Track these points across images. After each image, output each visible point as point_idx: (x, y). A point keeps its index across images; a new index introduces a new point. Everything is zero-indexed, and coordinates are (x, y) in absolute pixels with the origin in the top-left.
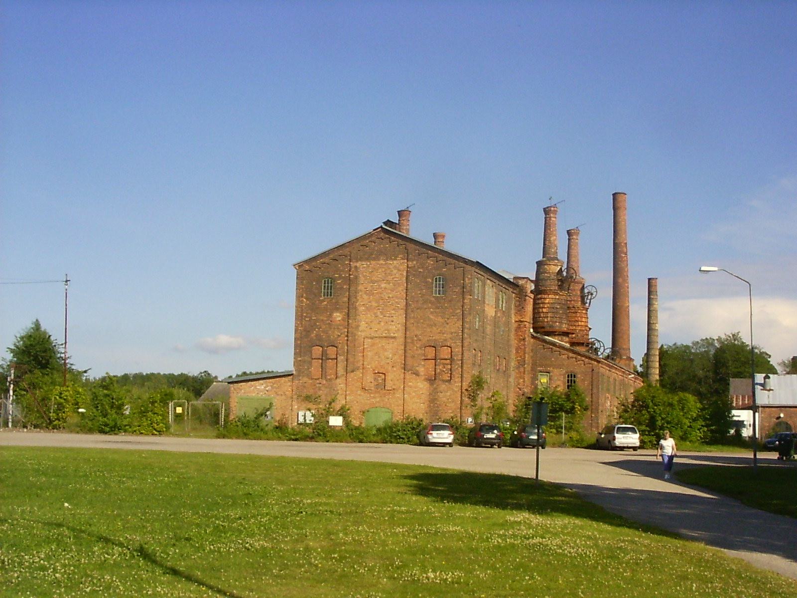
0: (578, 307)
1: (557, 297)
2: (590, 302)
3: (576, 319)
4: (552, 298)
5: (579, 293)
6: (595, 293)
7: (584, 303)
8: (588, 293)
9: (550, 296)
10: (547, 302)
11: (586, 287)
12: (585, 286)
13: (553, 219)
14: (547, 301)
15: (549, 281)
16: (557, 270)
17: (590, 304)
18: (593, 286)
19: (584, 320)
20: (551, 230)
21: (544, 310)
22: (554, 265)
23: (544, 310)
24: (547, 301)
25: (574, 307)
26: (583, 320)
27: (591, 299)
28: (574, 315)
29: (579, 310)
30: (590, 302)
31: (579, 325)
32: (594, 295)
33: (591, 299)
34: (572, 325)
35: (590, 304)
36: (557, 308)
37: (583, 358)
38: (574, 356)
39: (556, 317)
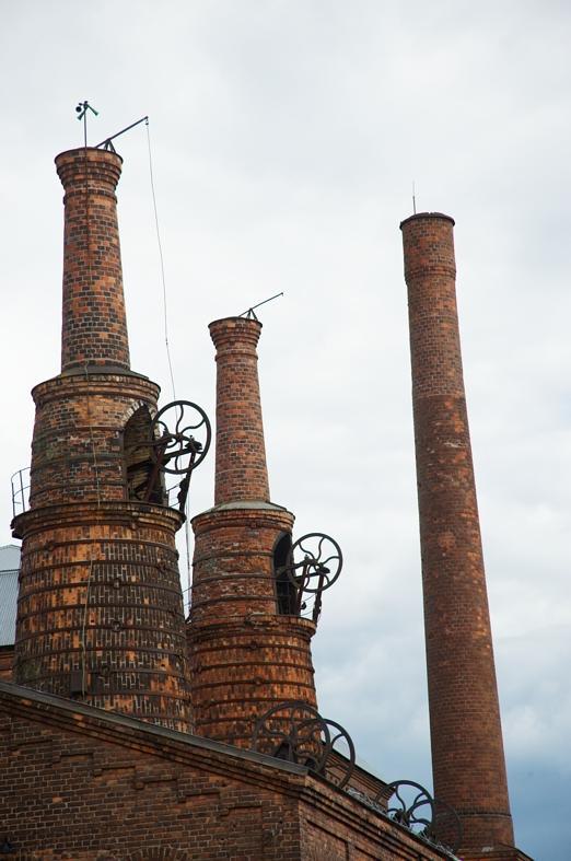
0: (266, 624)
1: (129, 536)
2: (318, 603)
3: (261, 672)
4: (102, 542)
5: (267, 565)
6: (332, 566)
7: (290, 604)
8: (307, 562)
10: (80, 558)
11: (299, 542)
12: (294, 540)
13: (98, 201)
14: (81, 554)
15: (85, 466)
16: (126, 418)
17: (317, 612)
18: (324, 536)
19: (292, 675)
20: (94, 247)
21: (70, 597)
22: (106, 395)
23: (70, 597)
24: (81, 554)
25: (248, 624)
26: (289, 678)
27: (321, 588)
28: (250, 657)
29: (268, 634)
30: (318, 603)
32: (331, 576)
33: (318, 592)
34: (241, 701)
35: (317, 612)
36: (128, 584)
37: (213, 779)
38: (166, 770)
39: (125, 628)
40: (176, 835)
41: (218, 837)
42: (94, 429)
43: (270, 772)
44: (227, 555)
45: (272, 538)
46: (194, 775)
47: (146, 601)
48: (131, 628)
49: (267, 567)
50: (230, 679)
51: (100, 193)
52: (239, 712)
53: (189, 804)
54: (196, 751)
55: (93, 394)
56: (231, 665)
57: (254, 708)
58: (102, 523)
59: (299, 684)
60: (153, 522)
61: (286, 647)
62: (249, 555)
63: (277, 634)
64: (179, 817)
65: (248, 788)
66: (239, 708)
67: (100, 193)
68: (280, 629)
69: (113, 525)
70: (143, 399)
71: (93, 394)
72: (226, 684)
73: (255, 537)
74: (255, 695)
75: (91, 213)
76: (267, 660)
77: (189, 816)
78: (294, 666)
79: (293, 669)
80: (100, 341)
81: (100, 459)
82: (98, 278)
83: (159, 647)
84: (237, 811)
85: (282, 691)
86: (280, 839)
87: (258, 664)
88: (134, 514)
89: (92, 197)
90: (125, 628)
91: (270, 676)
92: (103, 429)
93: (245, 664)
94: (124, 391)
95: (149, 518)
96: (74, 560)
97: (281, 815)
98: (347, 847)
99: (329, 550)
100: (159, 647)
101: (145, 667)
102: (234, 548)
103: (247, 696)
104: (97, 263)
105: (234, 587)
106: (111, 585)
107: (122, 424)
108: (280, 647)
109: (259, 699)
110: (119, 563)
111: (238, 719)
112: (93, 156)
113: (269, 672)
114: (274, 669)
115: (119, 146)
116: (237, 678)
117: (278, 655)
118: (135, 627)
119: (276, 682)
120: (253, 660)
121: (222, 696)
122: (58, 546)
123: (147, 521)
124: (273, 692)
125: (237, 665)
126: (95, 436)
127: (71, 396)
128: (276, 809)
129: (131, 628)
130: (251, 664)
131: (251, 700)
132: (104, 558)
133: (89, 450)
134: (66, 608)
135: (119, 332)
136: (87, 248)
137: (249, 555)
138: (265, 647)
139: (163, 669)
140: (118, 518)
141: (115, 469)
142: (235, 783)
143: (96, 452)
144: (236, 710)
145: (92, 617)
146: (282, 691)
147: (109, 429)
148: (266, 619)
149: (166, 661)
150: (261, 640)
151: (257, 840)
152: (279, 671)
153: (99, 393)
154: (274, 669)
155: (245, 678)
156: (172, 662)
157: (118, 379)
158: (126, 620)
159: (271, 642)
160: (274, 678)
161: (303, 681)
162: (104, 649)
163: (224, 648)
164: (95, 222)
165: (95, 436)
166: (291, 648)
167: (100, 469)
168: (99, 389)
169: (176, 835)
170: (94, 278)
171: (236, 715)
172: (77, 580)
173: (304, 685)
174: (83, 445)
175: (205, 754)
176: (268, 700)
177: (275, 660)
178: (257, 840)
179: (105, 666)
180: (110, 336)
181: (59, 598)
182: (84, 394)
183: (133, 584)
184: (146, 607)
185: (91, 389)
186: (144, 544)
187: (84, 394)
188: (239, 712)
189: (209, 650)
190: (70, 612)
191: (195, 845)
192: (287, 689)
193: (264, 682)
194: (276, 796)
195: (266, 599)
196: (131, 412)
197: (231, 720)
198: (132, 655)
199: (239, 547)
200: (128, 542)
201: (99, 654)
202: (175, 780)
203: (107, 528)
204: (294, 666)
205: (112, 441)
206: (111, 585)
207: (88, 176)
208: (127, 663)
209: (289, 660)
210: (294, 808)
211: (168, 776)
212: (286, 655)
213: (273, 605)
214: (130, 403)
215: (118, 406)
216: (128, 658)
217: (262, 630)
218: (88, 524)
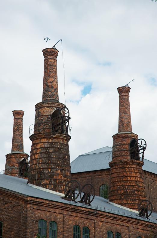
0: (126, 162)
1: (51, 141)
3: (125, 174)
4: (44, 143)
9: (43, 140)
10: (39, 147)
15: (42, 124)
16: (52, 112)
18: (143, 139)
20: (49, 72)
22: (47, 107)
25: (121, 162)
26: (133, 175)
28: (122, 170)
29: (127, 164)
31: (128, 181)
33: (143, 153)
34: (120, 181)
36: (50, 152)
37: (11, 199)
39: (48, 163)
40: (3, 213)
41: (11, 214)
42: (44, 115)
43: (21, 197)
44: (118, 145)
45: (130, 141)
46: (7, 198)
47: (54, 157)
48: (50, 163)
49: (128, 148)
50: (118, 176)
51: (51, 59)
52: (119, 184)
53: (6, 206)
54: (7, 192)
55: (44, 107)
56: (118, 172)
57: (123, 183)
58: (44, 138)
59: (135, 177)
60: (58, 137)
61: (132, 167)
62: (123, 145)
63: (129, 164)
64: (4, 209)
65: (18, 201)
66: (119, 183)
67: (51, 59)
68: (130, 163)
69: (46, 138)
70: (57, 107)
71: (44, 107)
72: (117, 177)
73: (125, 140)
74: (123, 180)
75: (48, 64)
76: (126, 171)
77: (6, 209)
78: (134, 172)
79: (134, 173)
80: (49, 94)
81: (45, 123)
82: (49, 79)
83: (57, 167)
84: (15, 207)
85: (130, 178)
86: (23, 213)
87: (124, 172)
88: (52, 135)
89: (49, 60)
90: (48, 163)
91: (127, 175)
92: (46, 115)
93: (121, 172)
94: (52, 106)
95: (56, 136)
96: (38, 147)
97: (24, 207)
98: (63, 215)
99: (144, 143)
100: (57, 167)
101: (53, 172)
102: (119, 144)
103: (121, 180)
104: (49, 75)
105: (119, 153)
106: (45, 153)
107: (51, 114)
108: (130, 167)
109: (124, 181)
110: (47, 147)
111: (119, 186)
112: (49, 50)
113: (127, 174)
114: (128, 173)
115: (57, 47)
116: (119, 176)
117: (129, 170)
118: (51, 163)
119: (129, 176)
120: (123, 171)
121: (116, 180)
122: (36, 144)
123: (56, 137)
124: (128, 179)
125: (119, 172)
126: (44, 117)
127: (40, 108)
128: (23, 206)
129: (50, 163)
130: (123, 172)
131: (122, 181)
132: (44, 147)
133: (43, 121)
134: (36, 159)
135: (54, 92)
136: (47, 72)
137: (123, 145)
138: (126, 167)
139: (58, 173)
140: (48, 136)
141: (48, 125)
142: (15, 200)
143: (44, 121)
144: (119, 183)
145: (41, 161)
146: (130, 178)
147: (47, 115)
148: (126, 161)
149: (59, 171)
150: (125, 166)
151: (19, 214)
152: (130, 174)
153: (46, 107)
154: (128, 173)
155: (121, 175)
156: (61, 171)
157: (50, 103)
158: (48, 161)
159: (128, 166)
160: (128, 175)
161: (137, 176)
162: (43, 168)
163: (116, 168)
164: (49, 66)
165: (44, 117)
166: (133, 168)
167: (45, 125)
168: (46, 106)
169: (3, 213)
170: (48, 79)
171: (119, 185)
172: (38, 152)
173: (138, 177)
174: (41, 119)
175: (8, 193)
176: (126, 181)
177: (129, 171)
178: (19, 214)
179: (43, 173)
180: (51, 93)
181: (35, 157)
182: (42, 107)
183: (51, 152)
184: (54, 158)
185: (44, 106)
186: (55, 143)
187: (42, 107)
188: (119, 184)
189: (113, 169)
190: (36, 160)
191: (6, 216)
192: (132, 178)
193: (126, 176)
194: (23, 203)
195: (127, 156)
196: (54, 111)
197: (118, 186)
198: (49, 170)
199: (121, 143)
200: (51, 142)
201: (42, 170)
202: (3, 200)
203: (45, 139)
204: (134, 172)
205: (48, 118)
206: (45, 153)
207: (50, 54)
208: (48, 172)
209: (133, 171)
210: (26, 206)
211: (2, 199)
212: (132, 169)
213: (129, 158)
214: (54, 109)
215: (50, 109)
216: (48, 171)
217: (125, 163)
218: (41, 139)
